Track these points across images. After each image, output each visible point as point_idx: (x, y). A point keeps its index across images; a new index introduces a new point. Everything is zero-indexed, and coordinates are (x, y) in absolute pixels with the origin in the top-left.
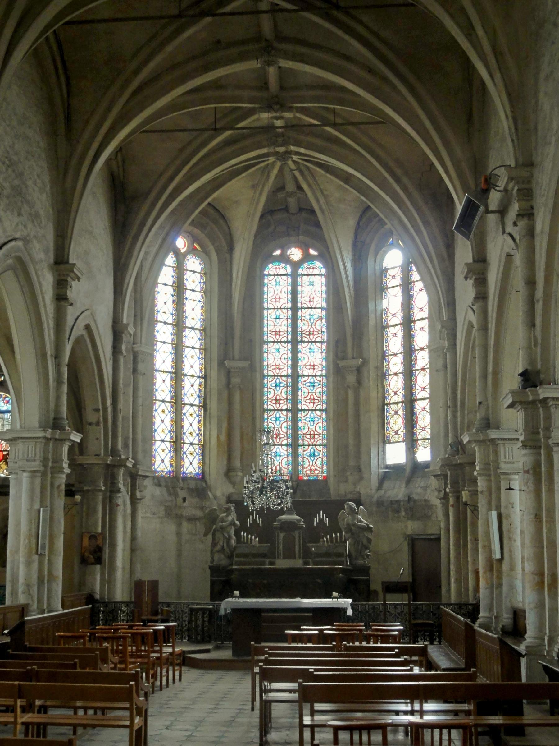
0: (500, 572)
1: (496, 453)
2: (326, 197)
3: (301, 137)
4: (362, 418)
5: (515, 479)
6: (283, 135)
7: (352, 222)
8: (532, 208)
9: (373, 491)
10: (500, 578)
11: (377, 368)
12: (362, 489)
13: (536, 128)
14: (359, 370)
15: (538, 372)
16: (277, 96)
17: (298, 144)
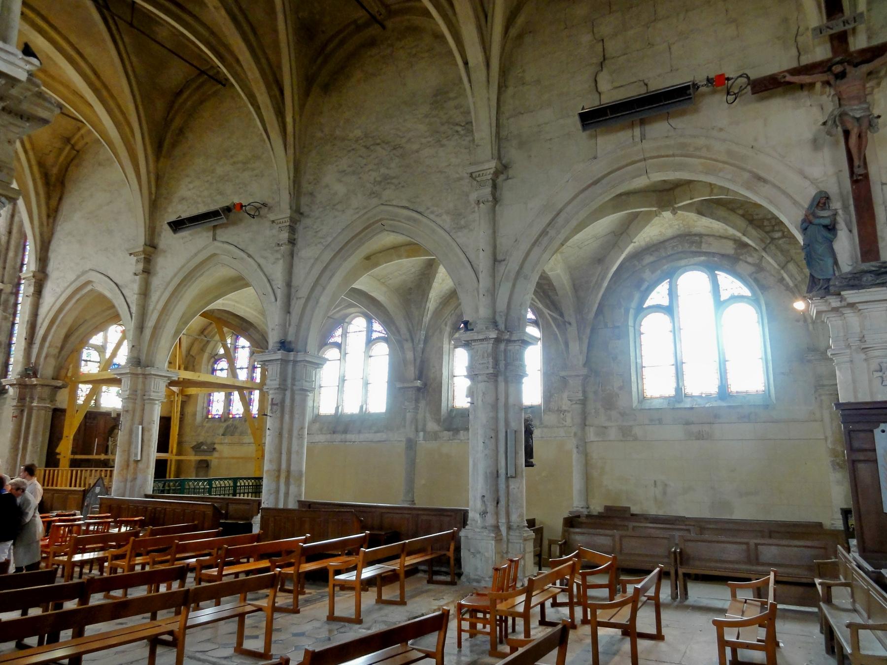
0: (135, 469)
1: (144, 383)
5: (156, 404)
8: (294, 240)
10: (135, 473)
15: (290, 342)
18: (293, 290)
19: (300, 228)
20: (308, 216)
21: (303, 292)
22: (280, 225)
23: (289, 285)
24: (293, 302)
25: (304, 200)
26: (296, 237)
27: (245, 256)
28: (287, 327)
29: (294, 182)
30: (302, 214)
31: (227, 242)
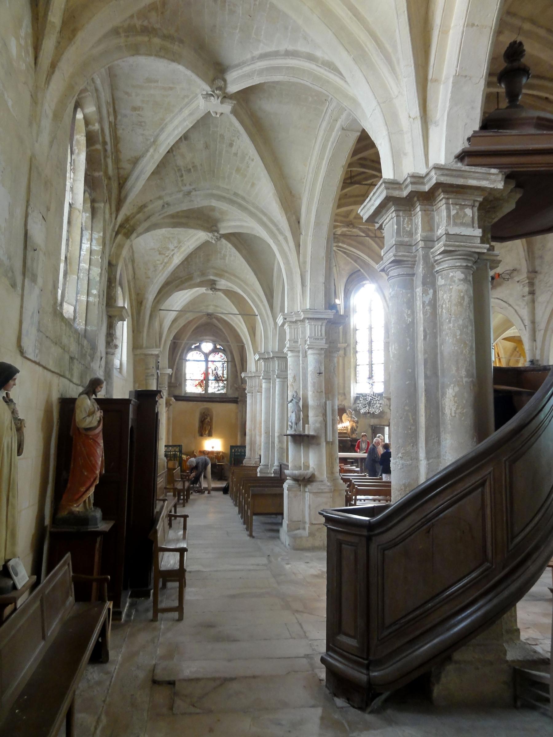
2: (339, 267)
3: (345, 240)
4: (346, 371)
6: (337, 238)
7: (345, 280)
8: (534, 291)
9: (352, 405)
11: (354, 348)
12: (346, 403)
13: (541, 257)
14: (345, 349)
15: (538, 361)
16: (351, 221)
17: (343, 242)
18: (536, 325)
19: (536, 281)
20: (541, 273)
21: (542, 326)
22: (523, 283)
23: (533, 322)
24: (537, 333)
25: (537, 262)
26: (535, 288)
27: (507, 305)
28: (535, 350)
29: (528, 252)
30: (536, 272)
31: (497, 298)
